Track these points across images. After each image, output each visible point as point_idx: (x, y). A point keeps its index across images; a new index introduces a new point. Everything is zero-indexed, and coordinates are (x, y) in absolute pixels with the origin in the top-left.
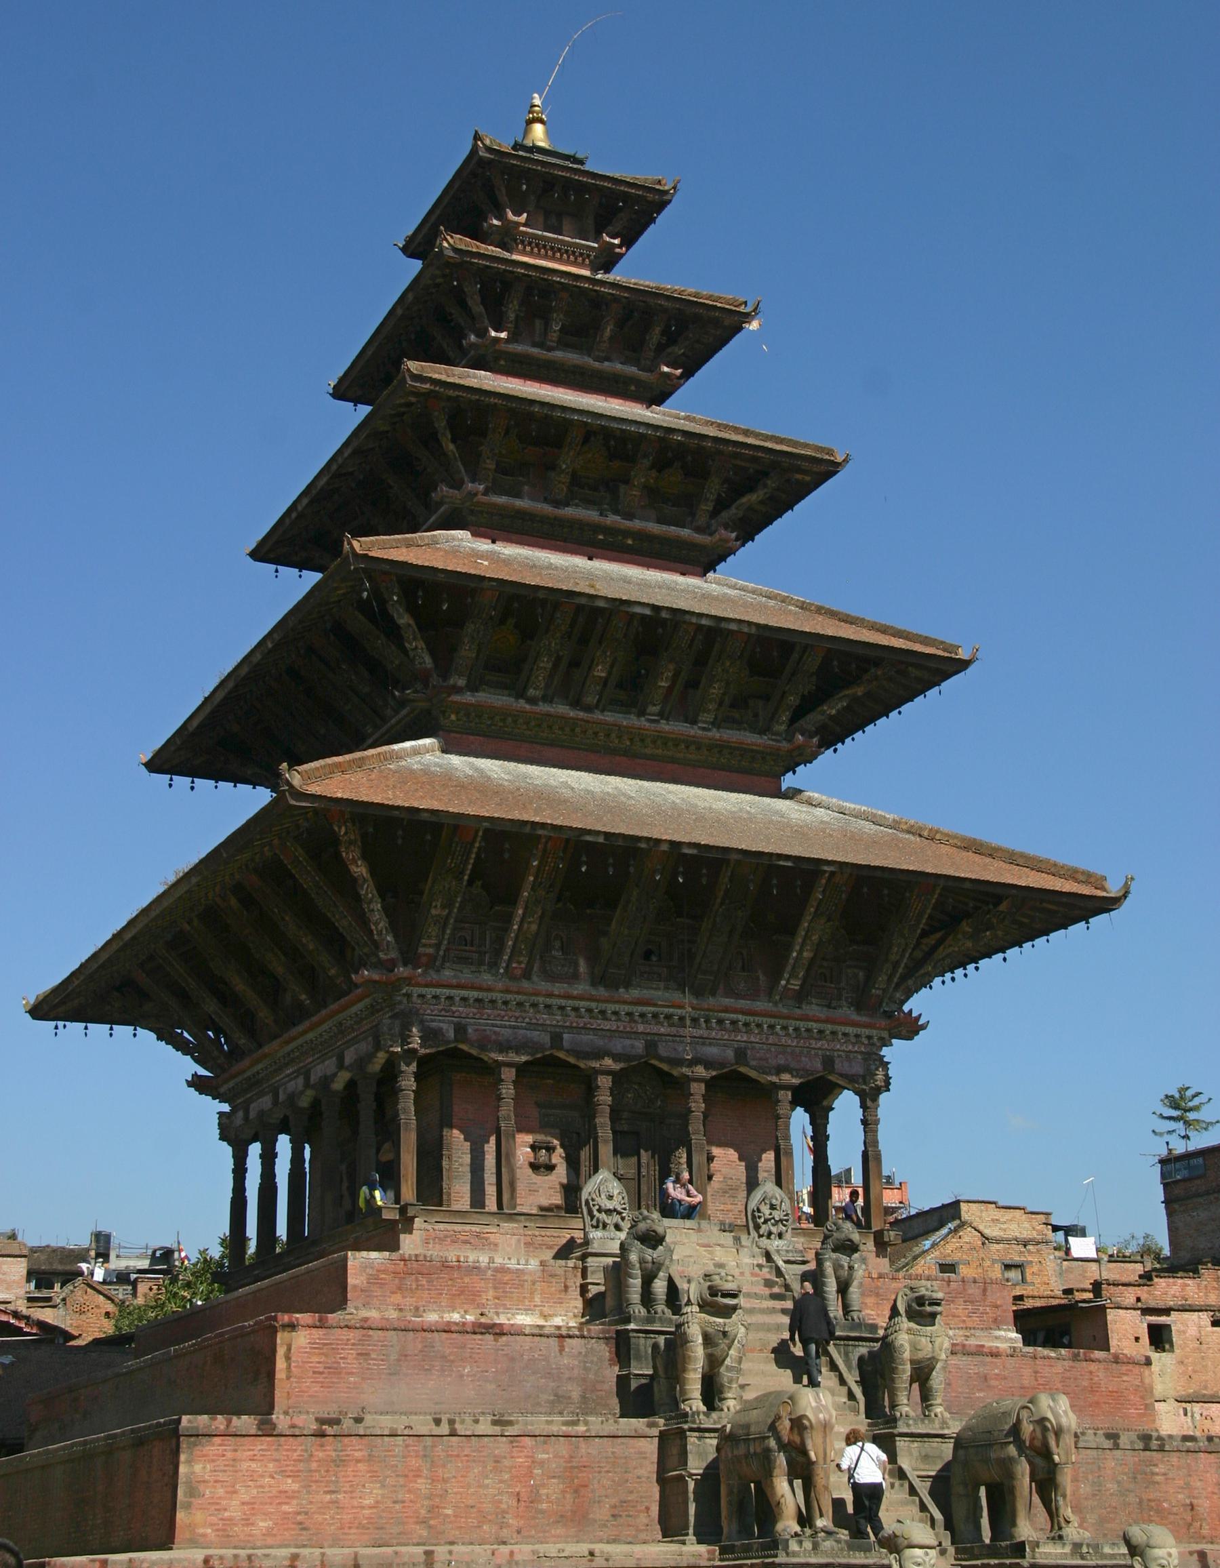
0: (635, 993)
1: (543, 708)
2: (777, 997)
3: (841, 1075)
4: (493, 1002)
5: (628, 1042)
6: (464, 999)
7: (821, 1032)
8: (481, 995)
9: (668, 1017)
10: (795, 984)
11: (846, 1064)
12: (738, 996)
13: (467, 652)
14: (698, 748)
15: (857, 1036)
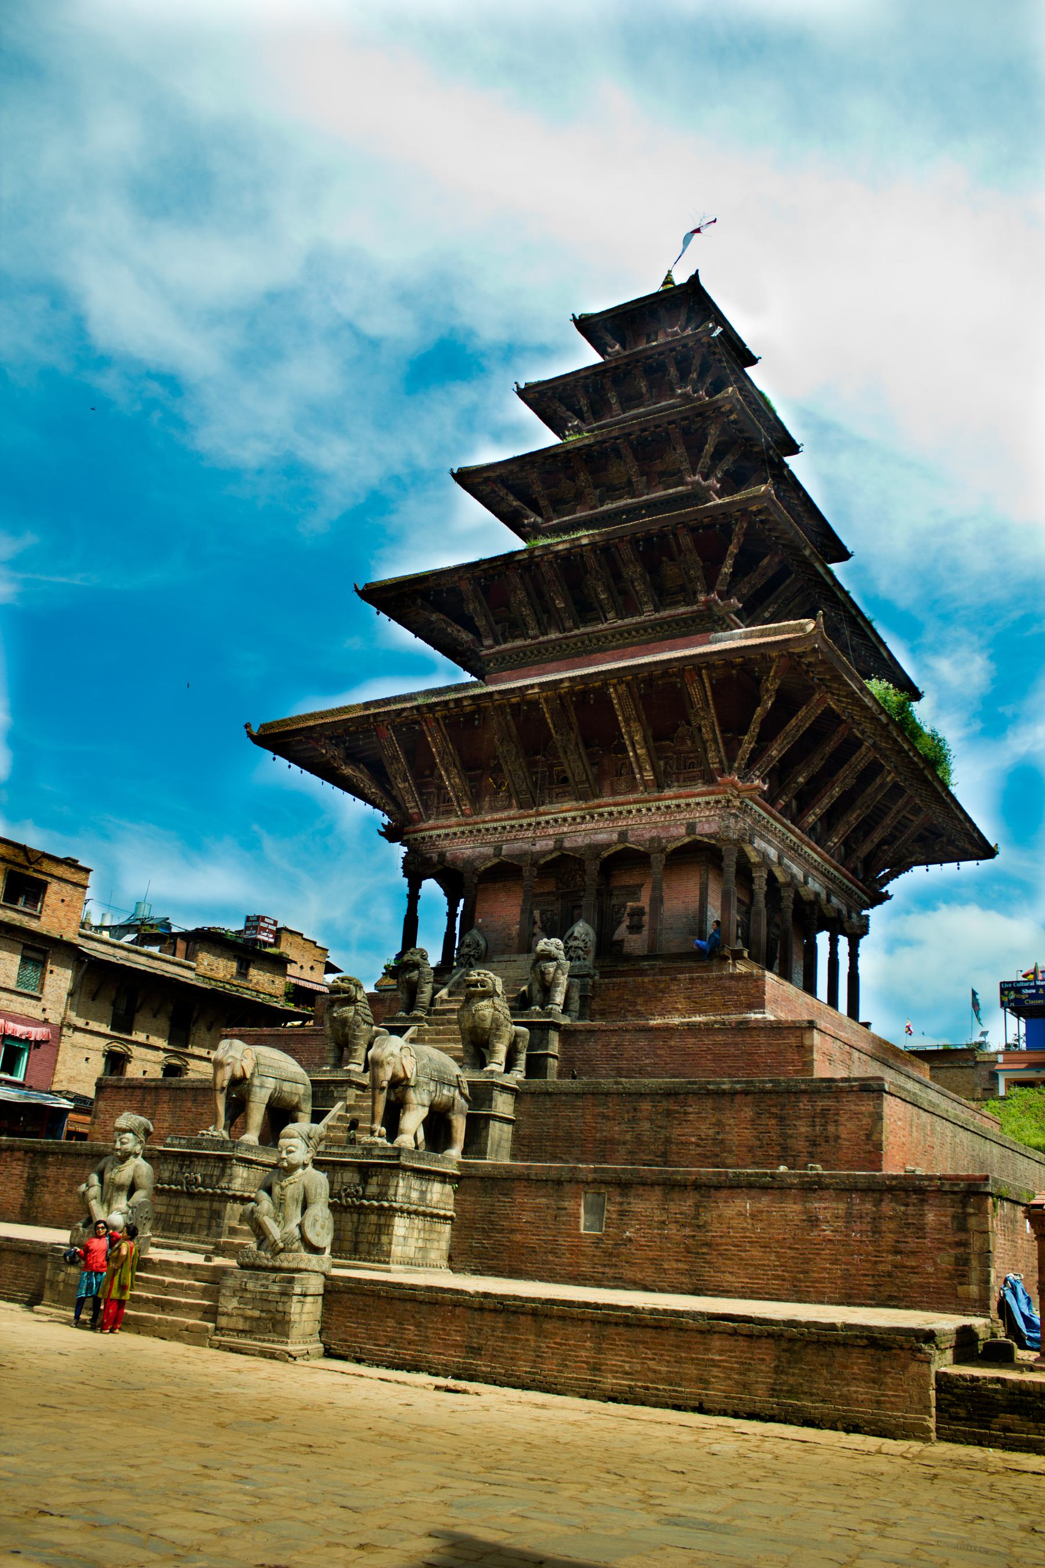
0: (542, 809)
1: (541, 639)
2: (641, 788)
3: (701, 835)
4: (455, 834)
5: (545, 842)
6: (439, 836)
7: (678, 806)
8: (447, 831)
9: (565, 820)
10: (649, 776)
11: (706, 826)
12: (621, 794)
13: (480, 622)
14: (645, 630)
15: (708, 803)
